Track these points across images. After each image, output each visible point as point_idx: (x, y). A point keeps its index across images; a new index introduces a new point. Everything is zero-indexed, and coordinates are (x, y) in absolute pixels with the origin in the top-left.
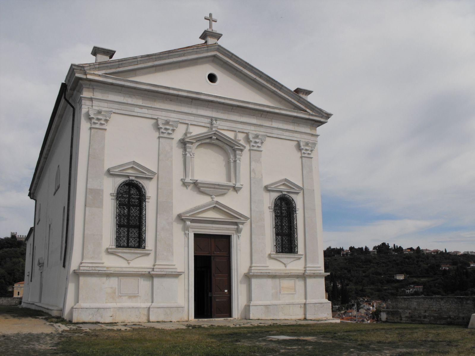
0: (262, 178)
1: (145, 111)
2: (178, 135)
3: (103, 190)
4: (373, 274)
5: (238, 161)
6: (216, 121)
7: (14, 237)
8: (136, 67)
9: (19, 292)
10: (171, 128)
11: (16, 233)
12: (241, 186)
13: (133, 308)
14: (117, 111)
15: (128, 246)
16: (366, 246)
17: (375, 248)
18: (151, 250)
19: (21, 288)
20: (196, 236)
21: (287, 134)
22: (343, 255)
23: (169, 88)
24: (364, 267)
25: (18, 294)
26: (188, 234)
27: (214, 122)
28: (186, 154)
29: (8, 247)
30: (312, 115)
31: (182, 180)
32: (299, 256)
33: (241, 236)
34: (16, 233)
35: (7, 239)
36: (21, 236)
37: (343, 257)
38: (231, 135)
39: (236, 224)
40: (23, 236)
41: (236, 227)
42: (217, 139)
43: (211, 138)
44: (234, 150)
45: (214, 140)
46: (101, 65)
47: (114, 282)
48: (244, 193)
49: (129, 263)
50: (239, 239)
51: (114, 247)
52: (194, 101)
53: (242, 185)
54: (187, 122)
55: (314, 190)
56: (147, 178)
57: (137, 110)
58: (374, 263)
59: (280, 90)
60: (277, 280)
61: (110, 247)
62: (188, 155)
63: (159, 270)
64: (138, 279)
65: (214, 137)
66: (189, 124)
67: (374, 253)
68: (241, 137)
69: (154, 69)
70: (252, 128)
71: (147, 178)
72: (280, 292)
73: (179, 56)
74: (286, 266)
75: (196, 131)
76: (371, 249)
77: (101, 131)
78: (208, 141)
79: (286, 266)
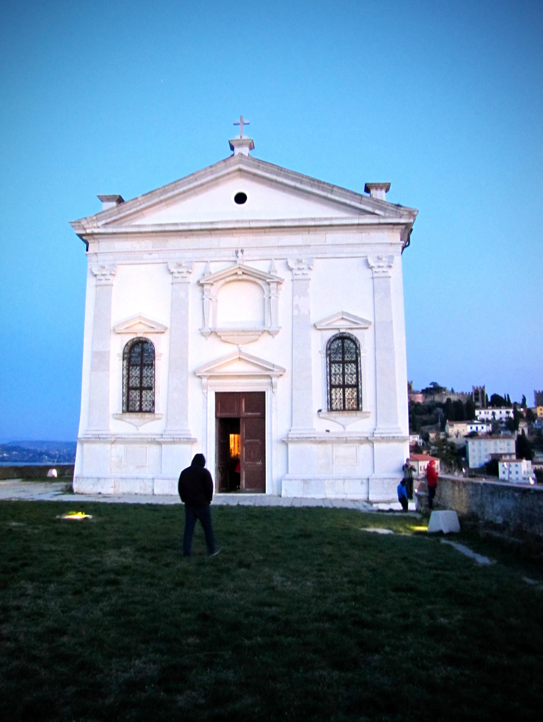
0: (310, 313)
1: (155, 255)
2: (193, 279)
3: (109, 352)
5: (273, 298)
6: (242, 251)
8: (139, 208)
10: (185, 270)
12: (278, 329)
13: (137, 478)
14: (124, 262)
15: (141, 411)
16: (535, 392)
18: (162, 415)
20: (217, 394)
21: (349, 249)
23: (176, 224)
26: (207, 393)
27: (240, 254)
28: (203, 299)
30: (384, 217)
31: (200, 330)
32: (363, 414)
33: (276, 392)
38: (262, 267)
39: (269, 377)
41: (269, 380)
42: (243, 273)
43: (236, 274)
44: (269, 284)
45: (240, 275)
46: (99, 216)
47: (119, 449)
48: (284, 336)
49: (138, 429)
50: (274, 396)
51: (121, 412)
52: (212, 232)
53: (280, 327)
54: (205, 260)
55: (392, 322)
56: (157, 333)
57: (146, 256)
59: (331, 194)
60: (329, 446)
61: (117, 412)
62: (206, 299)
63: (169, 436)
64: (146, 447)
65: (240, 272)
66: (209, 261)
68: (279, 266)
69: (164, 204)
70: (296, 251)
71: (157, 333)
72: (333, 463)
73: (190, 183)
74: (345, 429)
75: (215, 268)
77: (106, 288)
78: (235, 277)
79: (345, 429)
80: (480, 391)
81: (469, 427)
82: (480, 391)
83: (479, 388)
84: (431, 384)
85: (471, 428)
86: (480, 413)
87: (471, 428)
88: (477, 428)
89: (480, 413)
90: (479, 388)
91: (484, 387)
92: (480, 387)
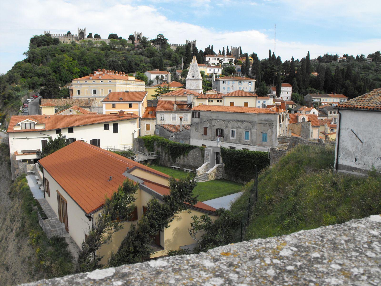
4: (373, 80)
7: (48, 35)
9: (79, 91)
11: (50, 32)
17: (369, 56)
19: (81, 85)
22: (340, 61)
24: (363, 73)
25: (79, 93)
29: (44, 45)
34: (50, 32)
35: (42, 36)
36: (54, 34)
37: (340, 64)
40: (57, 34)
58: (372, 70)
67: (369, 60)
76: (366, 57)
80: (192, 44)
81: (208, 69)
82: (192, 44)
83: (190, 42)
84: (158, 36)
85: (210, 70)
86: (209, 59)
87: (210, 70)
88: (214, 70)
89: (209, 59)
90: (190, 42)
91: (195, 41)
92: (192, 42)
